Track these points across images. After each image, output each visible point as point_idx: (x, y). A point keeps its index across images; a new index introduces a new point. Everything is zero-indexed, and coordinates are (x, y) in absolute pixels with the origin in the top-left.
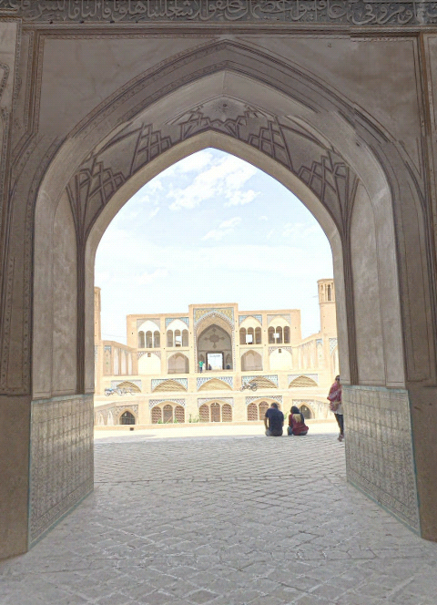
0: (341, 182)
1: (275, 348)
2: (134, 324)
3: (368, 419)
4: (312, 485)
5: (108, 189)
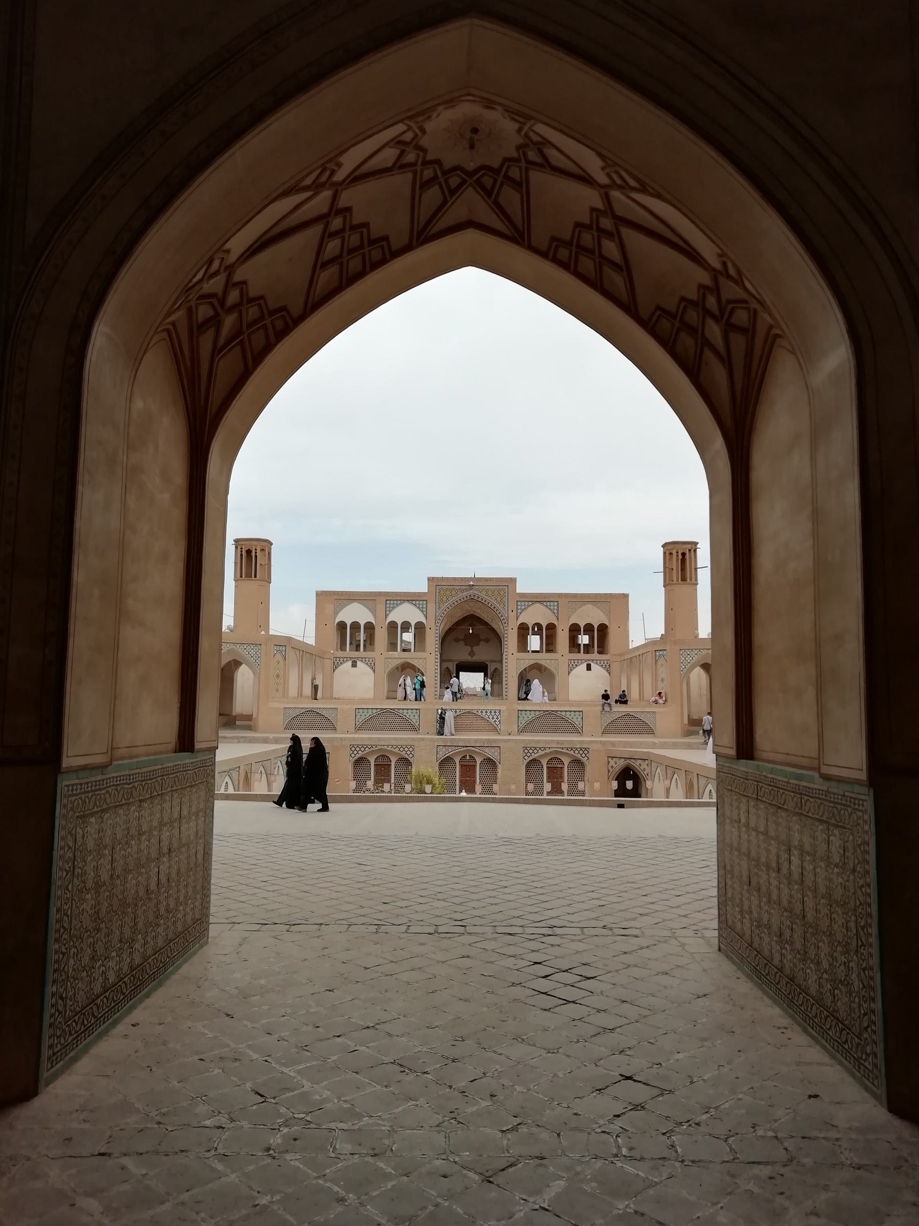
0: (738, 342)
1: (581, 661)
2: (329, 608)
3: (772, 833)
4: (645, 953)
5: (258, 340)
